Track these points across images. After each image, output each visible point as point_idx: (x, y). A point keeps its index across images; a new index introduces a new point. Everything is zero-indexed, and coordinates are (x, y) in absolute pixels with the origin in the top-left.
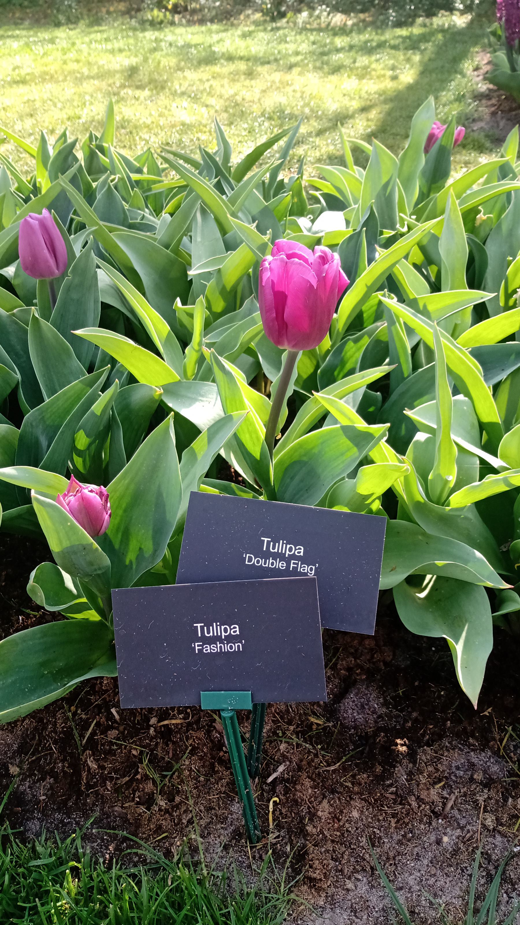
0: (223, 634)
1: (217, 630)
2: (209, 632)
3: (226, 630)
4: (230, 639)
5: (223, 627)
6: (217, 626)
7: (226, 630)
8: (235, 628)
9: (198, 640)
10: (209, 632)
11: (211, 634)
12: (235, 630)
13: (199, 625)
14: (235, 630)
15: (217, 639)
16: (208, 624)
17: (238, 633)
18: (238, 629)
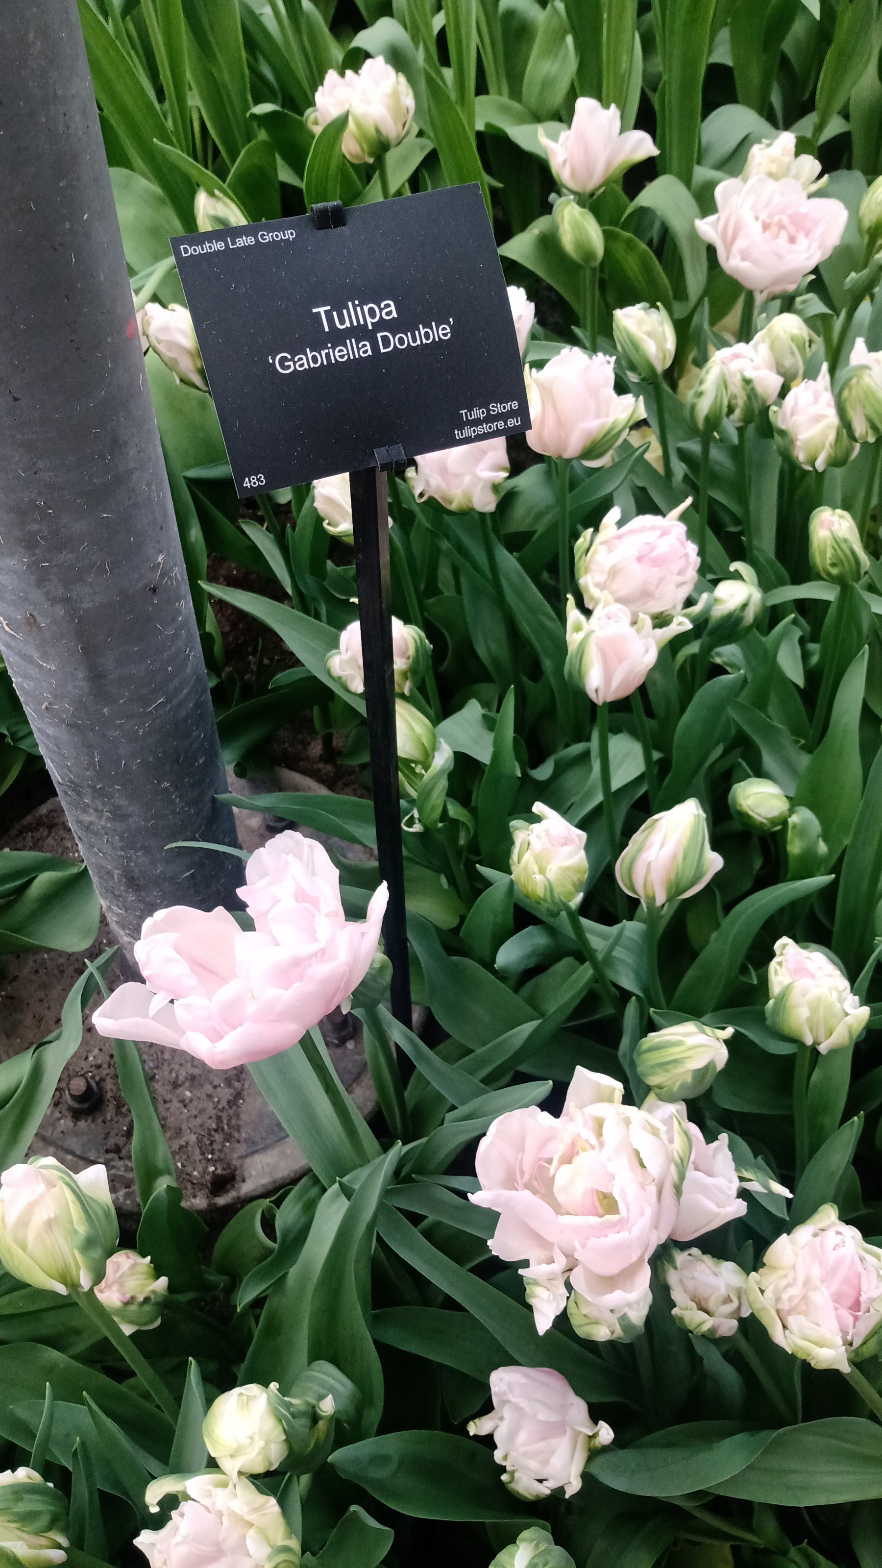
1: (357, 314)
2: (342, 322)
3: (372, 313)
5: (366, 308)
6: (354, 306)
7: (372, 313)
8: (388, 306)
10: (342, 322)
11: (348, 324)
12: (389, 310)
13: (322, 310)
14: (389, 310)
16: (339, 306)
17: (395, 314)
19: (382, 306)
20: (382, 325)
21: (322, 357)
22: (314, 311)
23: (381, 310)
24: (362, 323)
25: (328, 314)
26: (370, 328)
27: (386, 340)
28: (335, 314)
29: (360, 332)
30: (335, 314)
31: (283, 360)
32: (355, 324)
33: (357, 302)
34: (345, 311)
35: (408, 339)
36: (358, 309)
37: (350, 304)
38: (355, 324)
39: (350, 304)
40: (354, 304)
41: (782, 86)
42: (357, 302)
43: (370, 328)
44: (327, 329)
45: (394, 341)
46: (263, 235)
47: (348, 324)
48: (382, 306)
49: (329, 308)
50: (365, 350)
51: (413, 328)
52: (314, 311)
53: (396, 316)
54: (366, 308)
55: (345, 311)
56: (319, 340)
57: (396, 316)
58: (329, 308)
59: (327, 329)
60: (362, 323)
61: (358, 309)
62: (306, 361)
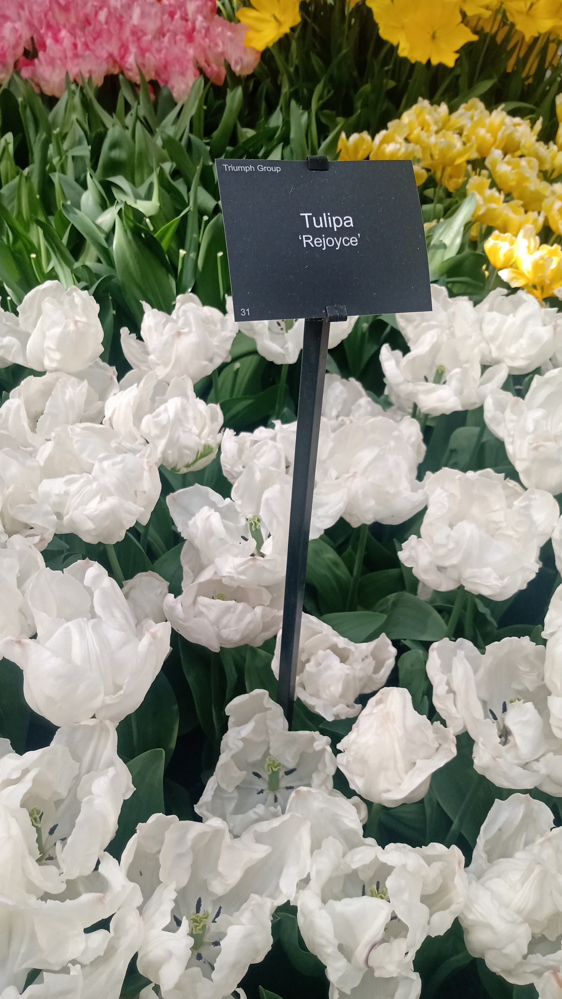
0: (335, 225)
1: (327, 221)
2: (318, 223)
3: (338, 222)
4: (343, 232)
5: (334, 219)
6: (327, 216)
7: (338, 222)
9: (308, 232)
10: (318, 223)
11: (321, 225)
12: (349, 222)
13: (306, 215)
14: (349, 222)
15: (328, 232)
16: (318, 214)
17: (352, 225)
18: (351, 221)
19: (345, 219)
22: (301, 214)
23: (343, 221)
24: (331, 226)
26: (335, 230)
28: (314, 218)
30: (314, 218)
32: (326, 226)
33: (329, 214)
34: (321, 218)
36: (329, 218)
37: (324, 214)
38: (326, 226)
39: (324, 214)
40: (327, 215)
41: (543, 123)
42: (329, 214)
43: (335, 230)
44: (308, 227)
46: (260, 167)
48: (345, 219)
49: (311, 214)
52: (301, 214)
53: (352, 226)
54: (334, 219)
55: (321, 218)
57: (352, 226)
58: (311, 214)
59: (308, 227)
60: (331, 226)
61: (329, 218)
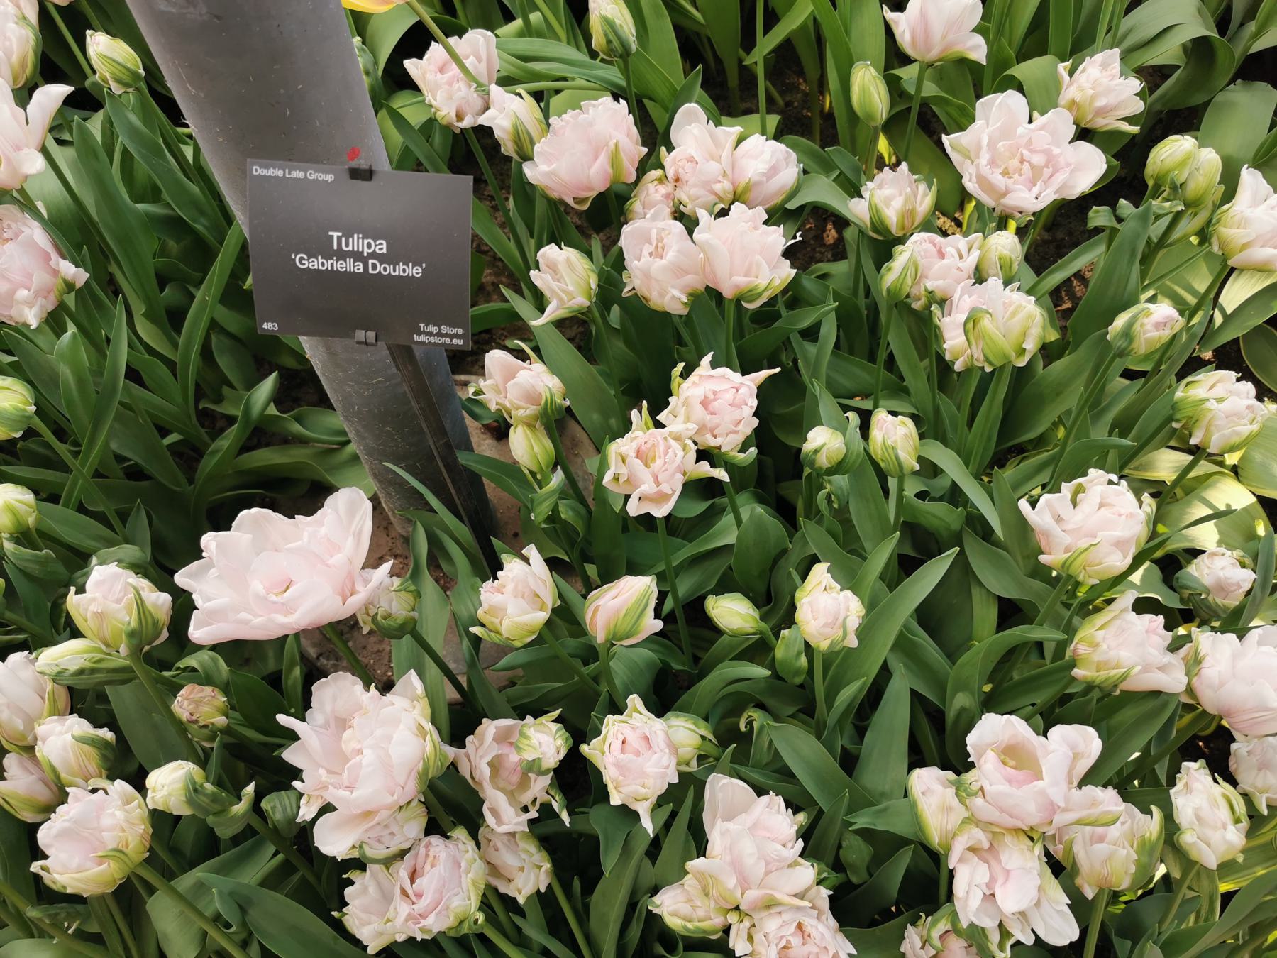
0: (366, 250)
2: (347, 245)
3: (369, 246)
7: (369, 246)
10: (347, 245)
12: (382, 247)
13: (335, 234)
14: (382, 247)
16: (348, 235)
17: (384, 251)
18: (384, 246)
20: (373, 255)
21: (328, 264)
25: (339, 238)
27: (374, 267)
29: (357, 256)
31: (301, 259)
35: (390, 269)
45: (380, 268)
47: (350, 248)
50: (359, 268)
51: (395, 264)
56: (328, 253)
62: (316, 264)
